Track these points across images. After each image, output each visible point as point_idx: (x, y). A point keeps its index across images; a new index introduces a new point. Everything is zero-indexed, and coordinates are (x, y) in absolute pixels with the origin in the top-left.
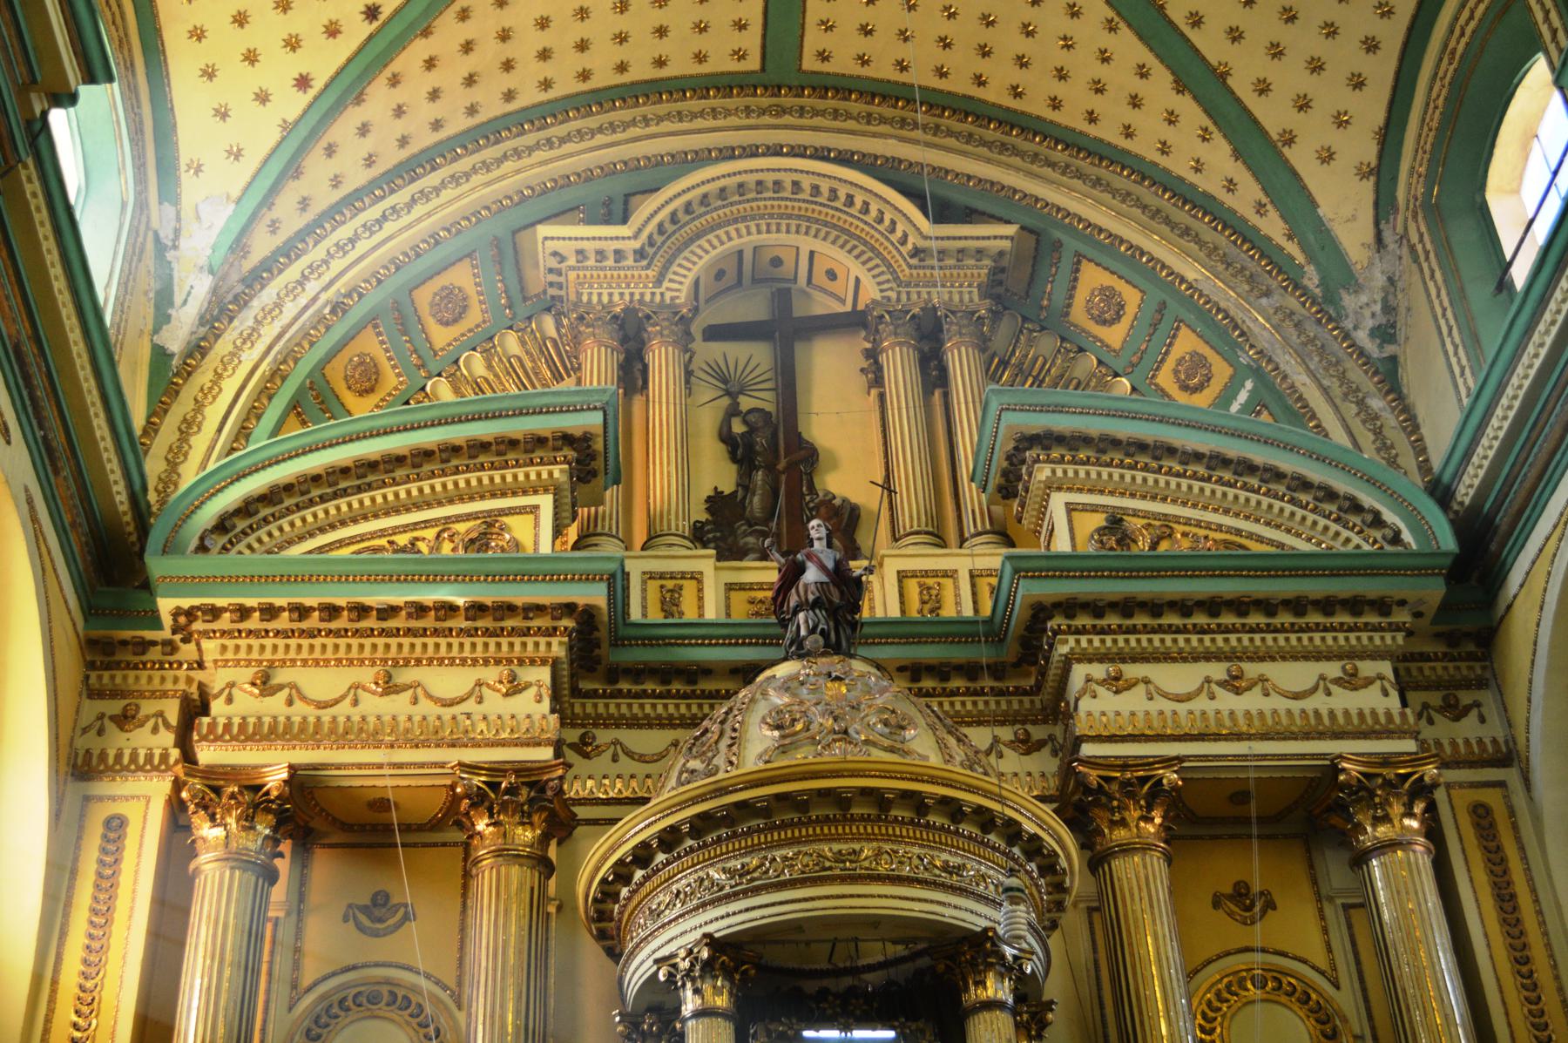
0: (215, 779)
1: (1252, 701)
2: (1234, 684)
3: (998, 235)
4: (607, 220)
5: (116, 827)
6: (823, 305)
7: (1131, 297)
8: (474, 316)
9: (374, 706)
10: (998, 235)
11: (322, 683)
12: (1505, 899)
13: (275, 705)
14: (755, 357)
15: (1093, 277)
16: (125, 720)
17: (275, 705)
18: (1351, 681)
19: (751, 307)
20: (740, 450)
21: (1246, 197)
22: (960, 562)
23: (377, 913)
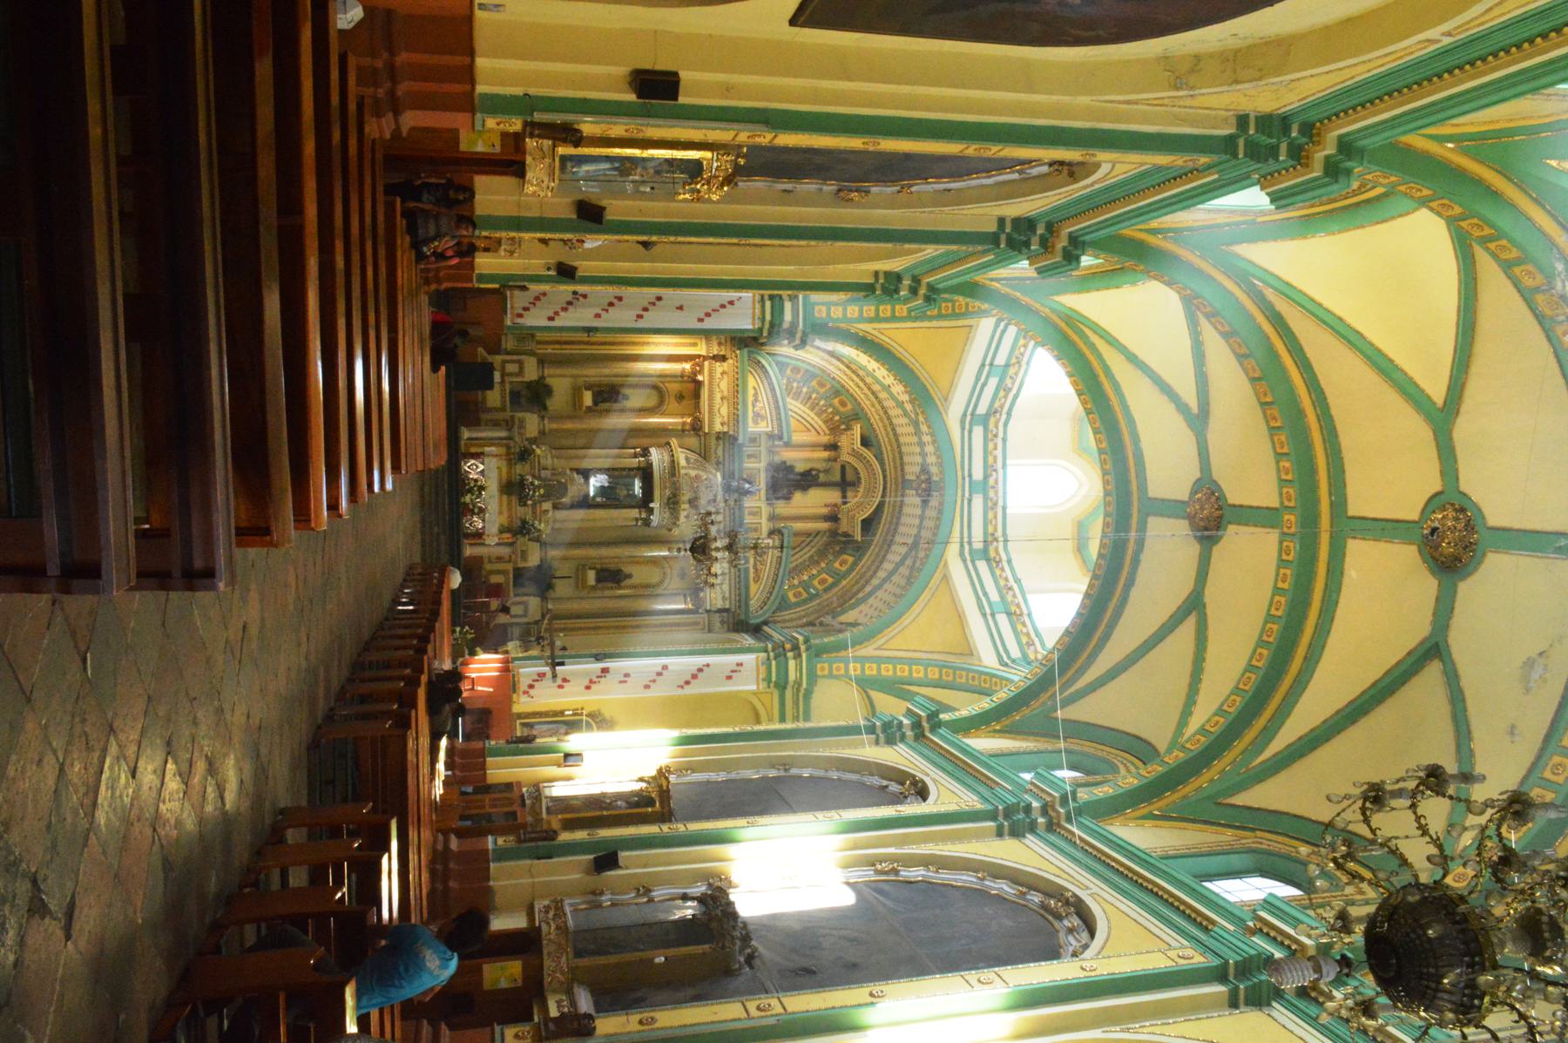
0: (702, 366)
3: (858, 537)
5: (695, 345)
6: (849, 494)
7: (844, 569)
9: (718, 396)
10: (858, 537)
11: (724, 385)
12: (678, 625)
13: (718, 375)
14: (837, 477)
15: (851, 559)
16: (720, 344)
17: (718, 375)
18: (724, 598)
19: (850, 476)
21: (861, 595)
22: (764, 521)
23: (680, 397)
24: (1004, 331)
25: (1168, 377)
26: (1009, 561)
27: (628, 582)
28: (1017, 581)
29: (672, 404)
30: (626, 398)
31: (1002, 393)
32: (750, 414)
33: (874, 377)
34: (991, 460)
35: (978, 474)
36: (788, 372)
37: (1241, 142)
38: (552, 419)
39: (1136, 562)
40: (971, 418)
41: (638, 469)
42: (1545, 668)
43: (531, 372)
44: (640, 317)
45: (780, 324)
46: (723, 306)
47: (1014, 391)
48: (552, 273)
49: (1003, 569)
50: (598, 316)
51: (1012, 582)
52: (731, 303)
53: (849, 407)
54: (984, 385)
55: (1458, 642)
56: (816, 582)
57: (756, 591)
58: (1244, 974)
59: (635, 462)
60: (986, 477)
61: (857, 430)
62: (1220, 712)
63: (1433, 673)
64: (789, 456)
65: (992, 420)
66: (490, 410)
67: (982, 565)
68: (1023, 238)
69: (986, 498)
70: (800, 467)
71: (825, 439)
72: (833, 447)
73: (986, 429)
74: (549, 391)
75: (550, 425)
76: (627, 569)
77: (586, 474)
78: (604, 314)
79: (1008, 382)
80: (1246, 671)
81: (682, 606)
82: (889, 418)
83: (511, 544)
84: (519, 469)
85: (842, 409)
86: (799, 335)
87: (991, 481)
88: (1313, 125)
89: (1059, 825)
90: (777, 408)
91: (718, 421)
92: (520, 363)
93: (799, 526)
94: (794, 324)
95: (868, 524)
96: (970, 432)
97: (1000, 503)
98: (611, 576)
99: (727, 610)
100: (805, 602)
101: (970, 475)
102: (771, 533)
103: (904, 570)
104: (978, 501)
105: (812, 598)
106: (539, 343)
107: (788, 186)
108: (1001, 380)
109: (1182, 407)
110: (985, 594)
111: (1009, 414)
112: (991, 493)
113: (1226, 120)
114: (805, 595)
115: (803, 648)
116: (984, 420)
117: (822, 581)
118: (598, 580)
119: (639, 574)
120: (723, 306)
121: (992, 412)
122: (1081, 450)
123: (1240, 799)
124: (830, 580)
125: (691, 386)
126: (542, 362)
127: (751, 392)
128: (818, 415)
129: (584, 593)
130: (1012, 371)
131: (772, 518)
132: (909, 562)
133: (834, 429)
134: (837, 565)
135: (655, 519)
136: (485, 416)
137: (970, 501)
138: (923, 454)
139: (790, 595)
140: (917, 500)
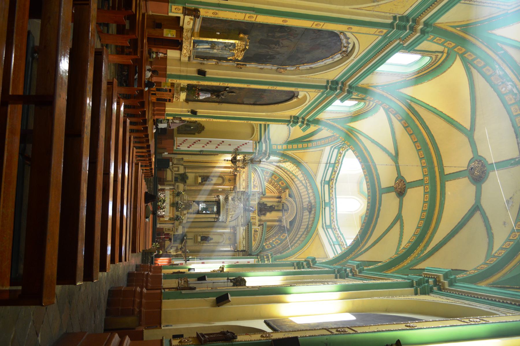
1: (242, 239)
2: (243, 238)
4: (289, 194)
7: (284, 238)
8: (282, 186)
9: (242, 179)
10: (288, 227)
18: (244, 247)
19: (285, 208)
20: (271, 207)
22: (257, 221)
23: (230, 180)
24: (333, 151)
25: (384, 145)
26: (339, 228)
27: (211, 241)
28: (342, 234)
29: (227, 182)
30: (212, 180)
31: (334, 173)
32: (252, 186)
33: (293, 174)
34: (331, 196)
35: (327, 200)
36: (265, 173)
37: (395, 24)
38: (188, 186)
39: (379, 210)
40: (324, 182)
41: (215, 201)
42: (513, 202)
43: (182, 171)
44: (217, 147)
45: (262, 151)
46: (243, 145)
47: (337, 172)
48: (189, 113)
49: (337, 231)
50: (203, 147)
51: (340, 235)
52: (246, 144)
53: (285, 184)
54: (328, 170)
55: (485, 204)
56: (274, 243)
57: (254, 244)
58: (419, 285)
59: (214, 199)
60: (330, 201)
61: (287, 192)
62: (409, 242)
63: (477, 215)
64: (264, 200)
65: (331, 183)
66: (168, 181)
67: (330, 230)
68: (334, 86)
69: (330, 208)
70: (269, 204)
71: (277, 195)
72: (280, 197)
73: (329, 186)
74: (187, 178)
75: (187, 188)
76: (211, 236)
77: (198, 203)
78: (205, 146)
79: (335, 169)
80: (417, 229)
81: (229, 249)
82: (298, 188)
83: (173, 224)
84: (177, 199)
85: (282, 186)
86: (268, 154)
87: (332, 202)
88: (416, 20)
89: (356, 275)
90: (261, 183)
91: (242, 187)
92: (178, 167)
93: (268, 223)
94: (266, 151)
95: (291, 223)
96: (324, 186)
97: (335, 209)
98: (205, 239)
99: (244, 251)
100: (271, 249)
101: (324, 201)
102: (259, 226)
103: (304, 236)
104: (327, 209)
105: (273, 247)
106: (184, 162)
107: (262, 67)
108: (333, 169)
109: (390, 154)
110: (331, 239)
111: (336, 180)
112: (332, 206)
113: (390, 17)
114: (271, 247)
115: (270, 257)
116: (328, 183)
117: (276, 242)
118: (202, 240)
119: (215, 238)
120: (243, 145)
121: (331, 179)
122: (361, 192)
123: (417, 267)
124: (279, 242)
125: (233, 177)
126: (185, 168)
127: (252, 178)
128: (275, 188)
129: (197, 244)
130: (336, 165)
131: (260, 220)
132: (305, 233)
133: (280, 192)
134: (281, 237)
135: (221, 218)
136: (167, 183)
137: (325, 209)
138: (309, 197)
139: (266, 247)
140: (308, 213)
